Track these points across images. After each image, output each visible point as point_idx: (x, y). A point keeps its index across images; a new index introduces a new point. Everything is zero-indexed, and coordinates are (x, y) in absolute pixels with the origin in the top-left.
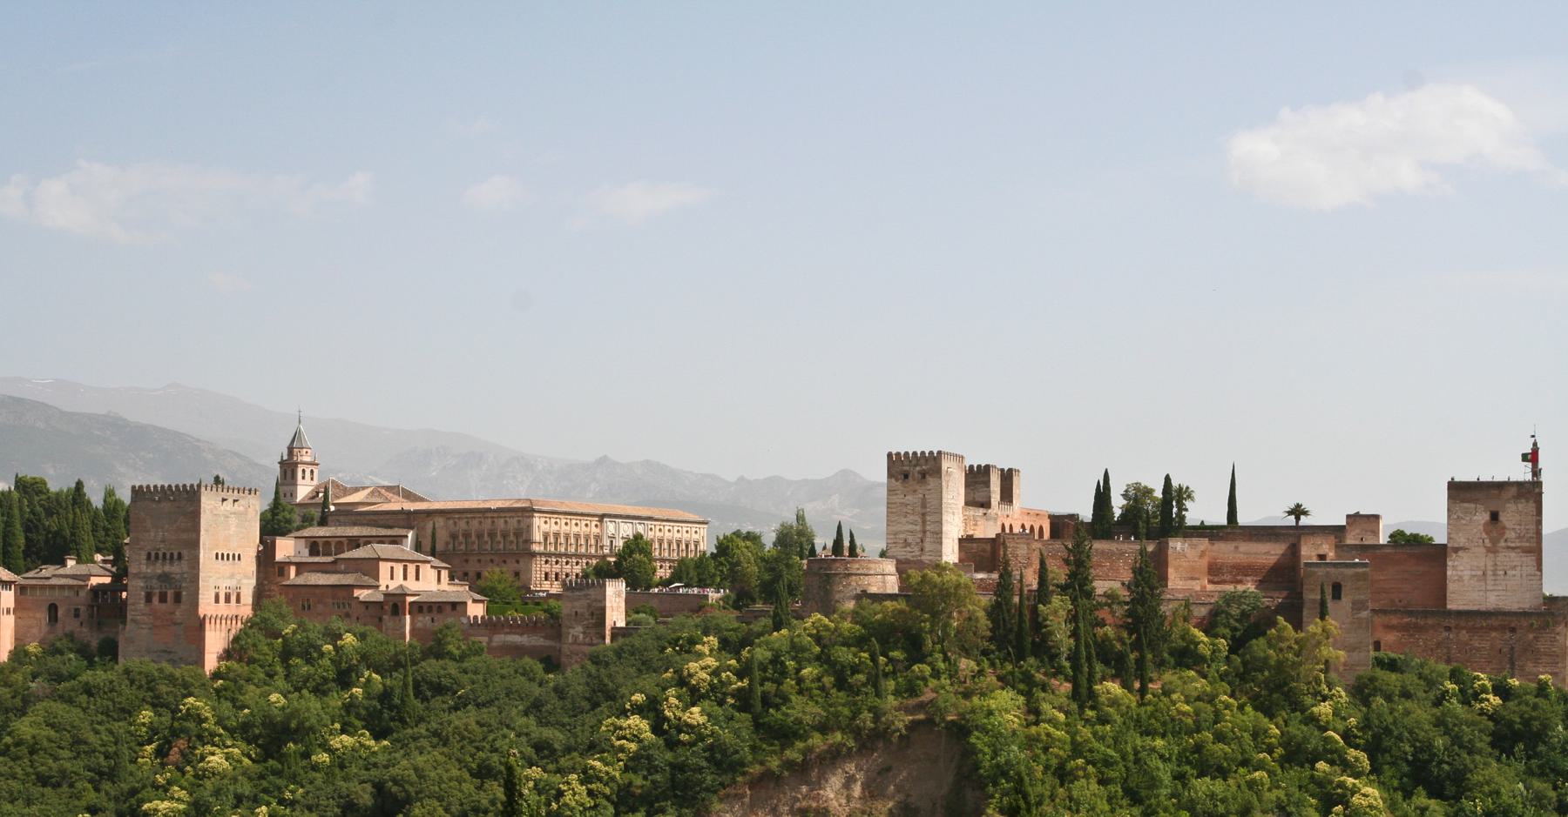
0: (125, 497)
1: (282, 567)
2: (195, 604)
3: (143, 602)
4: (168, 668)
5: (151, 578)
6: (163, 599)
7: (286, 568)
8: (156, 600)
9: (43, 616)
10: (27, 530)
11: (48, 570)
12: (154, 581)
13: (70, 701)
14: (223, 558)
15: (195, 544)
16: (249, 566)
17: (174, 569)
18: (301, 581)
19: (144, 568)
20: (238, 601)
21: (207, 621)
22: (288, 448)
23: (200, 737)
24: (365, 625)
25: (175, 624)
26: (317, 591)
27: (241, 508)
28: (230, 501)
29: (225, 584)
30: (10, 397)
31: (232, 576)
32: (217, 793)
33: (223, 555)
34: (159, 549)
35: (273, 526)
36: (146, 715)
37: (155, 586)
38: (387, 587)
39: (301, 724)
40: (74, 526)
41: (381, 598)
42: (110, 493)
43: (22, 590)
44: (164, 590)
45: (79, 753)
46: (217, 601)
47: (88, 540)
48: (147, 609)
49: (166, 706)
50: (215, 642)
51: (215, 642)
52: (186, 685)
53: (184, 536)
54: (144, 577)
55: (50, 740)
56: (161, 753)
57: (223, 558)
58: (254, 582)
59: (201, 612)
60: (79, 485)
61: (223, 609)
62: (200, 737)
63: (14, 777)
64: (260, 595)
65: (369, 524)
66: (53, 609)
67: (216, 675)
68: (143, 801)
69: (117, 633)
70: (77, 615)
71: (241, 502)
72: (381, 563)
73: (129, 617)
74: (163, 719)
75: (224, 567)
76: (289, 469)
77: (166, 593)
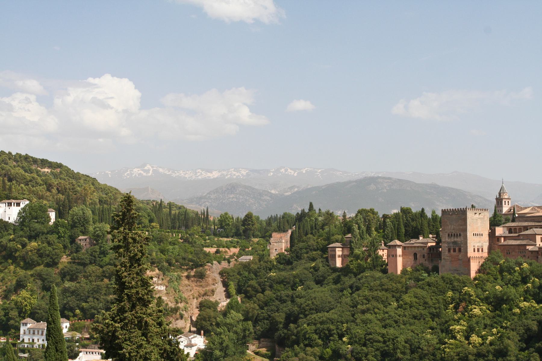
0: (439, 214)
1: (499, 238)
2: (466, 252)
3: (447, 252)
4: (457, 277)
5: (450, 243)
6: (454, 250)
7: (500, 238)
8: (452, 251)
9: (412, 257)
10: (405, 226)
11: (413, 241)
12: (451, 244)
13: (423, 288)
14: (476, 235)
15: (465, 230)
16: (486, 238)
17: (458, 239)
18: (506, 243)
19: (447, 239)
20: (482, 251)
21: (471, 259)
22: (499, 193)
23: (470, 302)
24: (531, 260)
25: (459, 260)
26: (512, 247)
27: (482, 216)
28: (478, 214)
29: (477, 245)
30: (398, 179)
31: (479, 242)
32: (477, 323)
33: (476, 234)
34: (452, 233)
35: (494, 223)
36: (450, 293)
37: (451, 246)
38: (540, 245)
39: (508, 297)
40: (422, 225)
41: (537, 249)
42: (434, 212)
43: (404, 248)
44: (455, 247)
45: (426, 307)
46: (474, 251)
47: (426, 229)
48: (449, 254)
49: (457, 290)
50: (474, 267)
51: (474, 267)
52: (464, 283)
53: (461, 227)
54: (447, 243)
55: (416, 303)
56: (456, 308)
57: (476, 235)
58: (488, 244)
59: (469, 255)
60: (423, 210)
61: (477, 254)
62: (470, 302)
63: (405, 316)
64: (490, 249)
65: (531, 221)
66: (415, 255)
67: (475, 279)
68: (449, 326)
69: (438, 264)
70: (424, 257)
71: (482, 214)
72: (537, 236)
73: (442, 258)
74: (456, 295)
75: (477, 238)
76: (499, 201)
77: (455, 249)
